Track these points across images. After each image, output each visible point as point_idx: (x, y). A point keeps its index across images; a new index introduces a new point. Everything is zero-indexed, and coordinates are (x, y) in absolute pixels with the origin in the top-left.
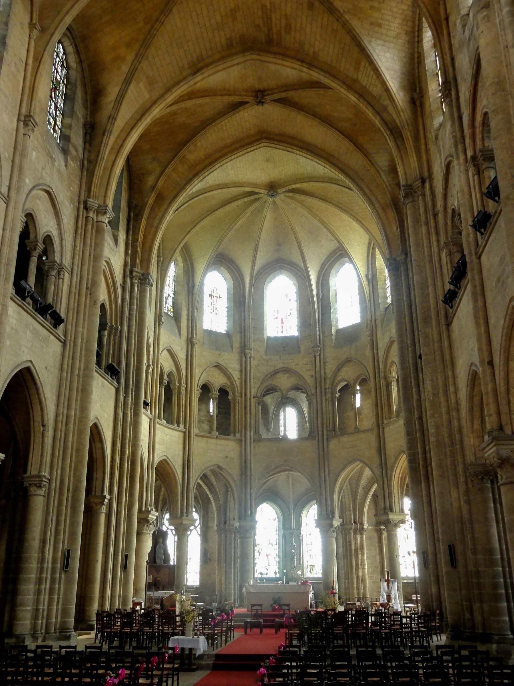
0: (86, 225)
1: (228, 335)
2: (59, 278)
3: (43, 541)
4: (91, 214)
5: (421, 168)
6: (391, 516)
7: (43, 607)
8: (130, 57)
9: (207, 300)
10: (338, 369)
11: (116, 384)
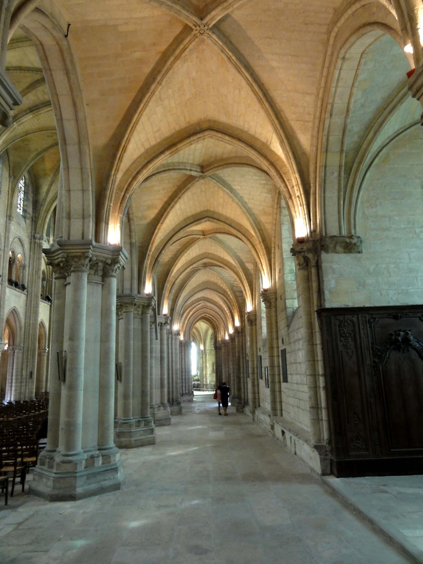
0: (35, 245)
2: (24, 270)
4: (37, 241)
8: (52, 175)
11: (50, 304)
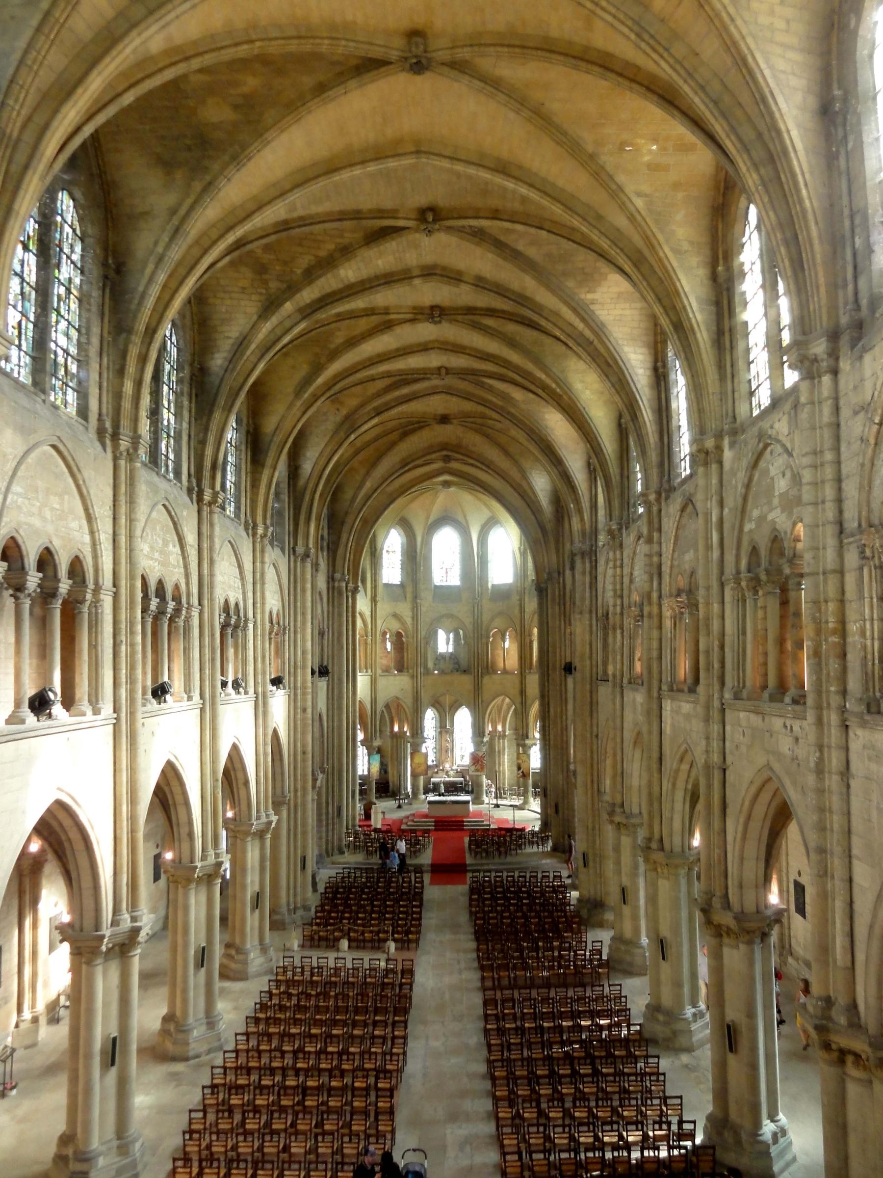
1: (402, 585)
3: (327, 803)
5: (558, 563)
6: (527, 742)
7: (330, 838)
9: (385, 555)
10: (492, 619)
